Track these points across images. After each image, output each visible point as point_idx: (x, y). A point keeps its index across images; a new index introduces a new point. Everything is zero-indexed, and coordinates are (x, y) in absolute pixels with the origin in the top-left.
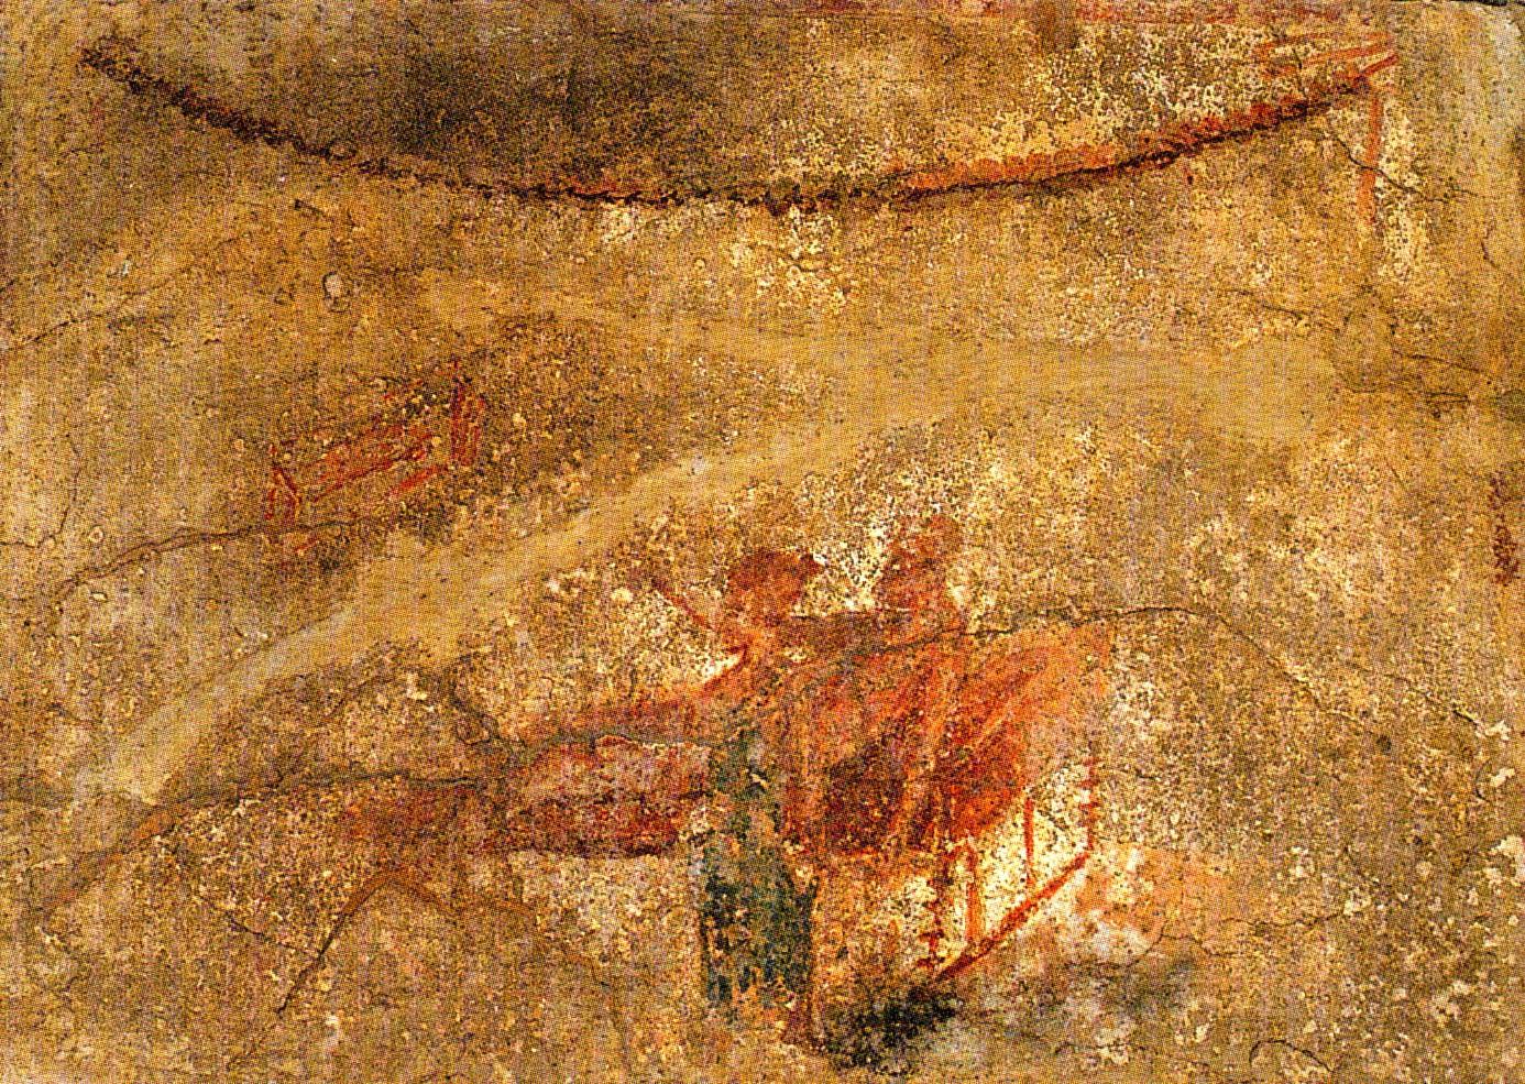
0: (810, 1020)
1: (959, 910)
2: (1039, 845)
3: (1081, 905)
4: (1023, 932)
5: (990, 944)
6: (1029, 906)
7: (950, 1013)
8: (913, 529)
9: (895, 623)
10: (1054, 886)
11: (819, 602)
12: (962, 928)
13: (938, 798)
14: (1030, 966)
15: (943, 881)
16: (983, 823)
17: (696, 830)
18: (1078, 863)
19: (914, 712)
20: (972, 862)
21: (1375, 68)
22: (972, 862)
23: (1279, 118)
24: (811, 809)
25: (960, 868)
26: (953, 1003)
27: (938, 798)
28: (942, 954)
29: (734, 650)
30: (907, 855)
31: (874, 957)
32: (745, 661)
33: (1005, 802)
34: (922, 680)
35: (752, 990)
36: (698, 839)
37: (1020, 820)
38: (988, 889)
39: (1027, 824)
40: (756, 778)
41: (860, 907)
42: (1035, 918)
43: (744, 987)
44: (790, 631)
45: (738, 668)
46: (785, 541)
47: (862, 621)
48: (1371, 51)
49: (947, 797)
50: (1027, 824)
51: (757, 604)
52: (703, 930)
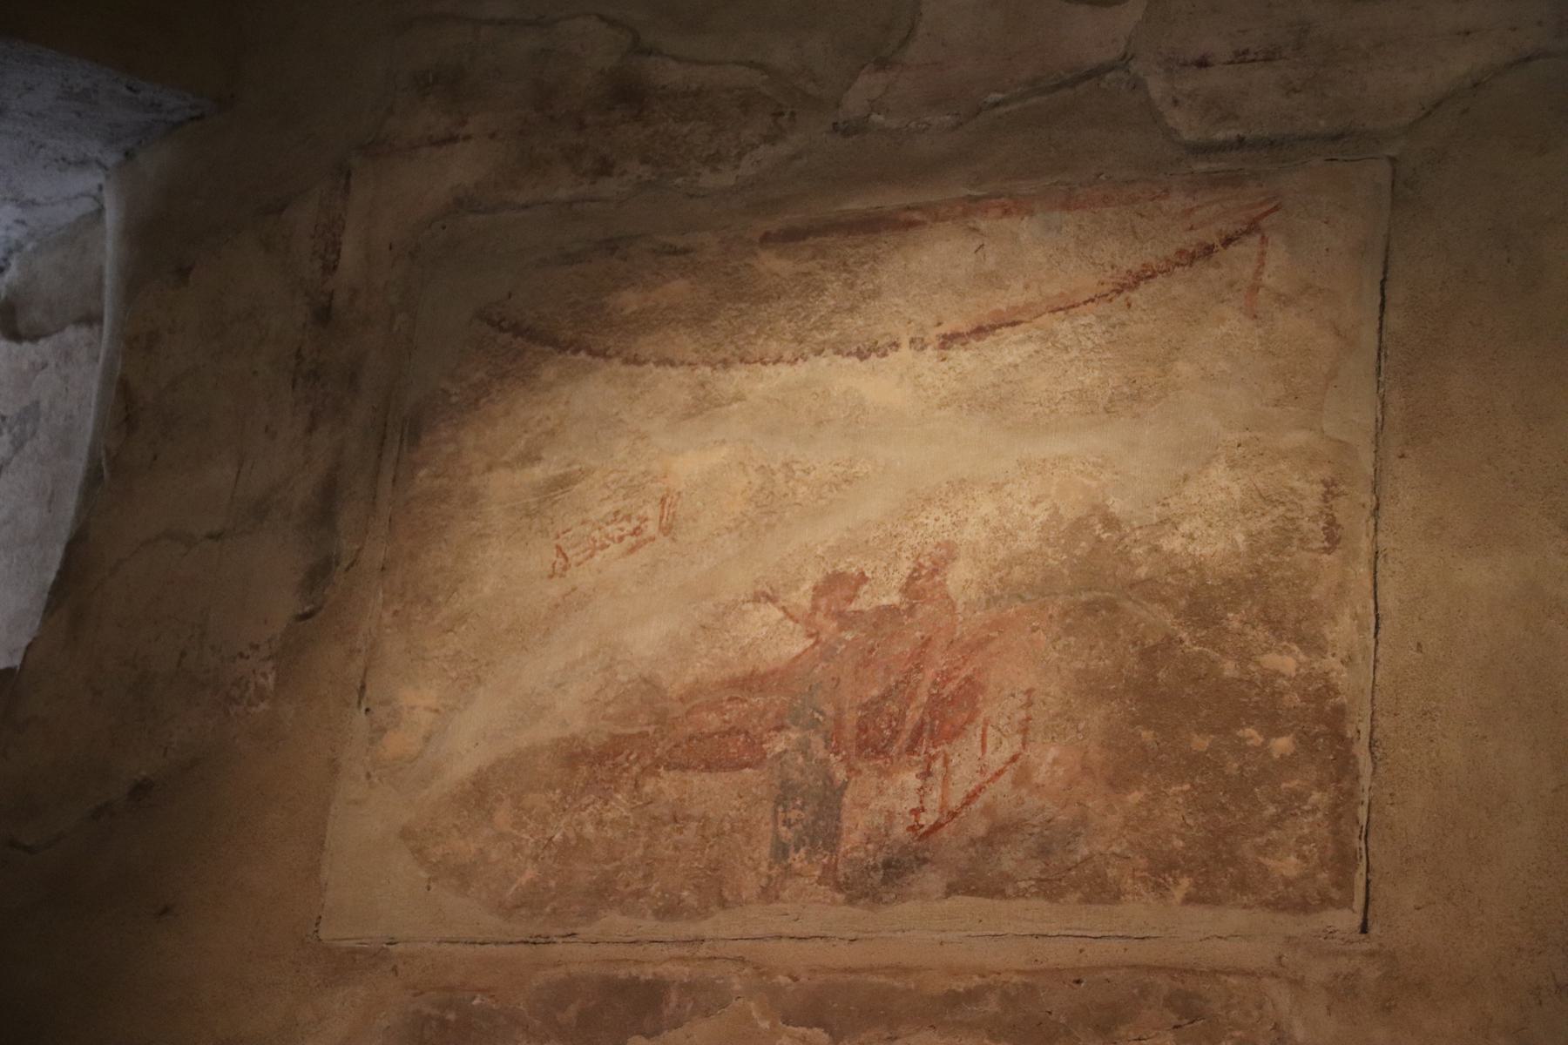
0: (836, 869)
1: (935, 795)
2: (990, 747)
3: (1016, 783)
4: (977, 805)
5: (954, 815)
6: (980, 789)
7: (925, 861)
8: (929, 549)
9: (911, 610)
10: (999, 774)
11: (865, 601)
12: (937, 806)
13: (928, 719)
14: (980, 828)
15: (927, 774)
16: (956, 735)
17: (778, 750)
18: (1014, 759)
19: (917, 666)
20: (946, 762)
21: (1266, 214)
22: (946, 762)
23: (1193, 258)
24: (849, 733)
25: (937, 766)
26: (927, 854)
27: (928, 719)
28: (922, 822)
29: (811, 636)
30: (905, 757)
31: (878, 828)
32: (817, 643)
33: (971, 720)
34: (925, 645)
35: (802, 850)
36: (779, 756)
37: (979, 732)
38: (955, 778)
39: (984, 736)
40: (816, 715)
41: (873, 793)
42: (984, 797)
43: (797, 850)
44: (845, 620)
45: (812, 646)
46: (851, 565)
47: (892, 610)
48: (1261, 204)
49: (934, 719)
50: (984, 736)
51: (828, 606)
52: (776, 812)
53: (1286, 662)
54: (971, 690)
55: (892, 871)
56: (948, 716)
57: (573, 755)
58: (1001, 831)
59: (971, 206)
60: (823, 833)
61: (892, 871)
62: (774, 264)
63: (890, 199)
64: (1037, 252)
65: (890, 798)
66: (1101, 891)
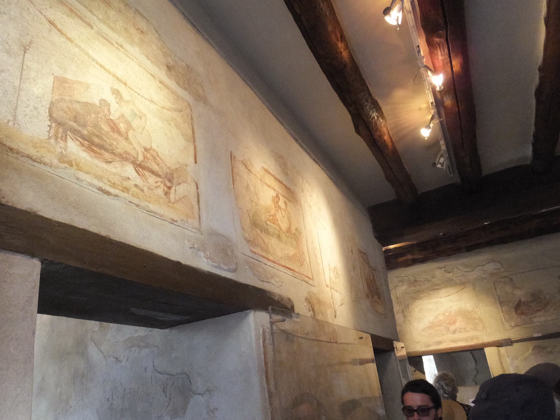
53: (476, 316)
54: (456, 320)
55: (455, 332)
56: (454, 322)
57: (428, 327)
58: (461, 329)
59: (445, 287)
60: (448, 330)
61: (455, 332)
62: (431, 292)
63: (438, 287)
64: (451, 290)
65: (452, 328)
66: (469, 332)
